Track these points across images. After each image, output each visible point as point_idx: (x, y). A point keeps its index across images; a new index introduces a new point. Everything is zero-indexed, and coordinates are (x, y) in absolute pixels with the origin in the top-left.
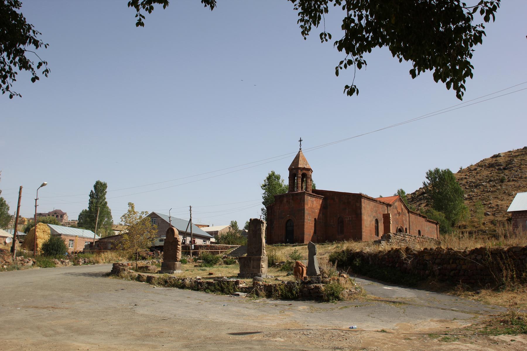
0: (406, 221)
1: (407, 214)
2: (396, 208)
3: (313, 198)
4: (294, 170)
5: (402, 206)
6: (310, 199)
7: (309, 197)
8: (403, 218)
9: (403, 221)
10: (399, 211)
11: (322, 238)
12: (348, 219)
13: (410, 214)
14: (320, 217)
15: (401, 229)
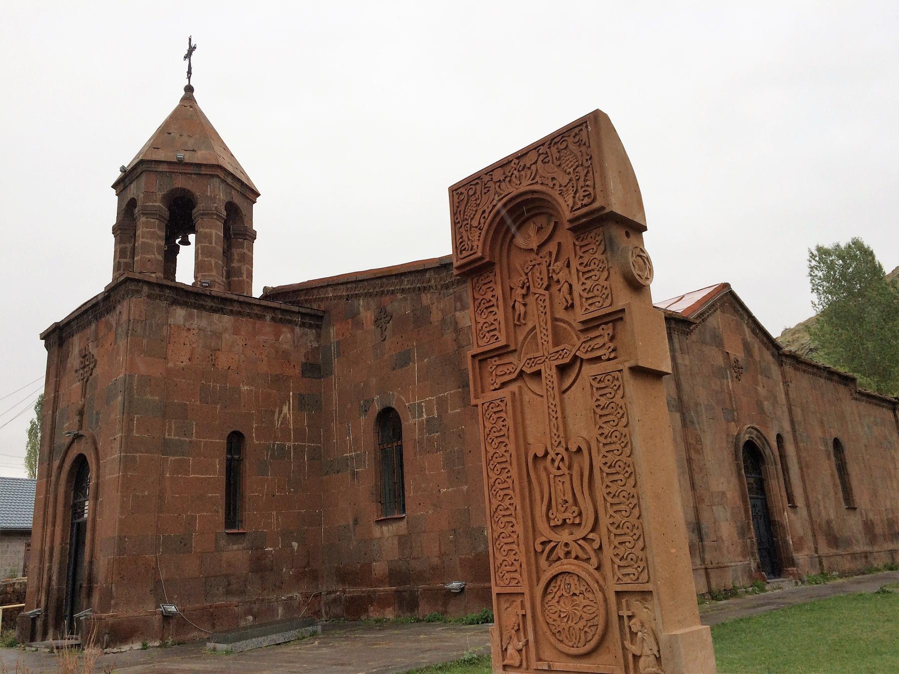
0: (775, 402)
1: (775, 370)
2: (719, 343)
3: (216, 316)
4: (132, 186)
5: (747, 331)
6: (186, 319)
7: (179, 314)
8: (760, 389)
9: (759, 405)
10: (732, 357)
11: (295, 545)
12: (425, 417)
13: (788, 368)
14: (278, 424)
15: (758, 443)
